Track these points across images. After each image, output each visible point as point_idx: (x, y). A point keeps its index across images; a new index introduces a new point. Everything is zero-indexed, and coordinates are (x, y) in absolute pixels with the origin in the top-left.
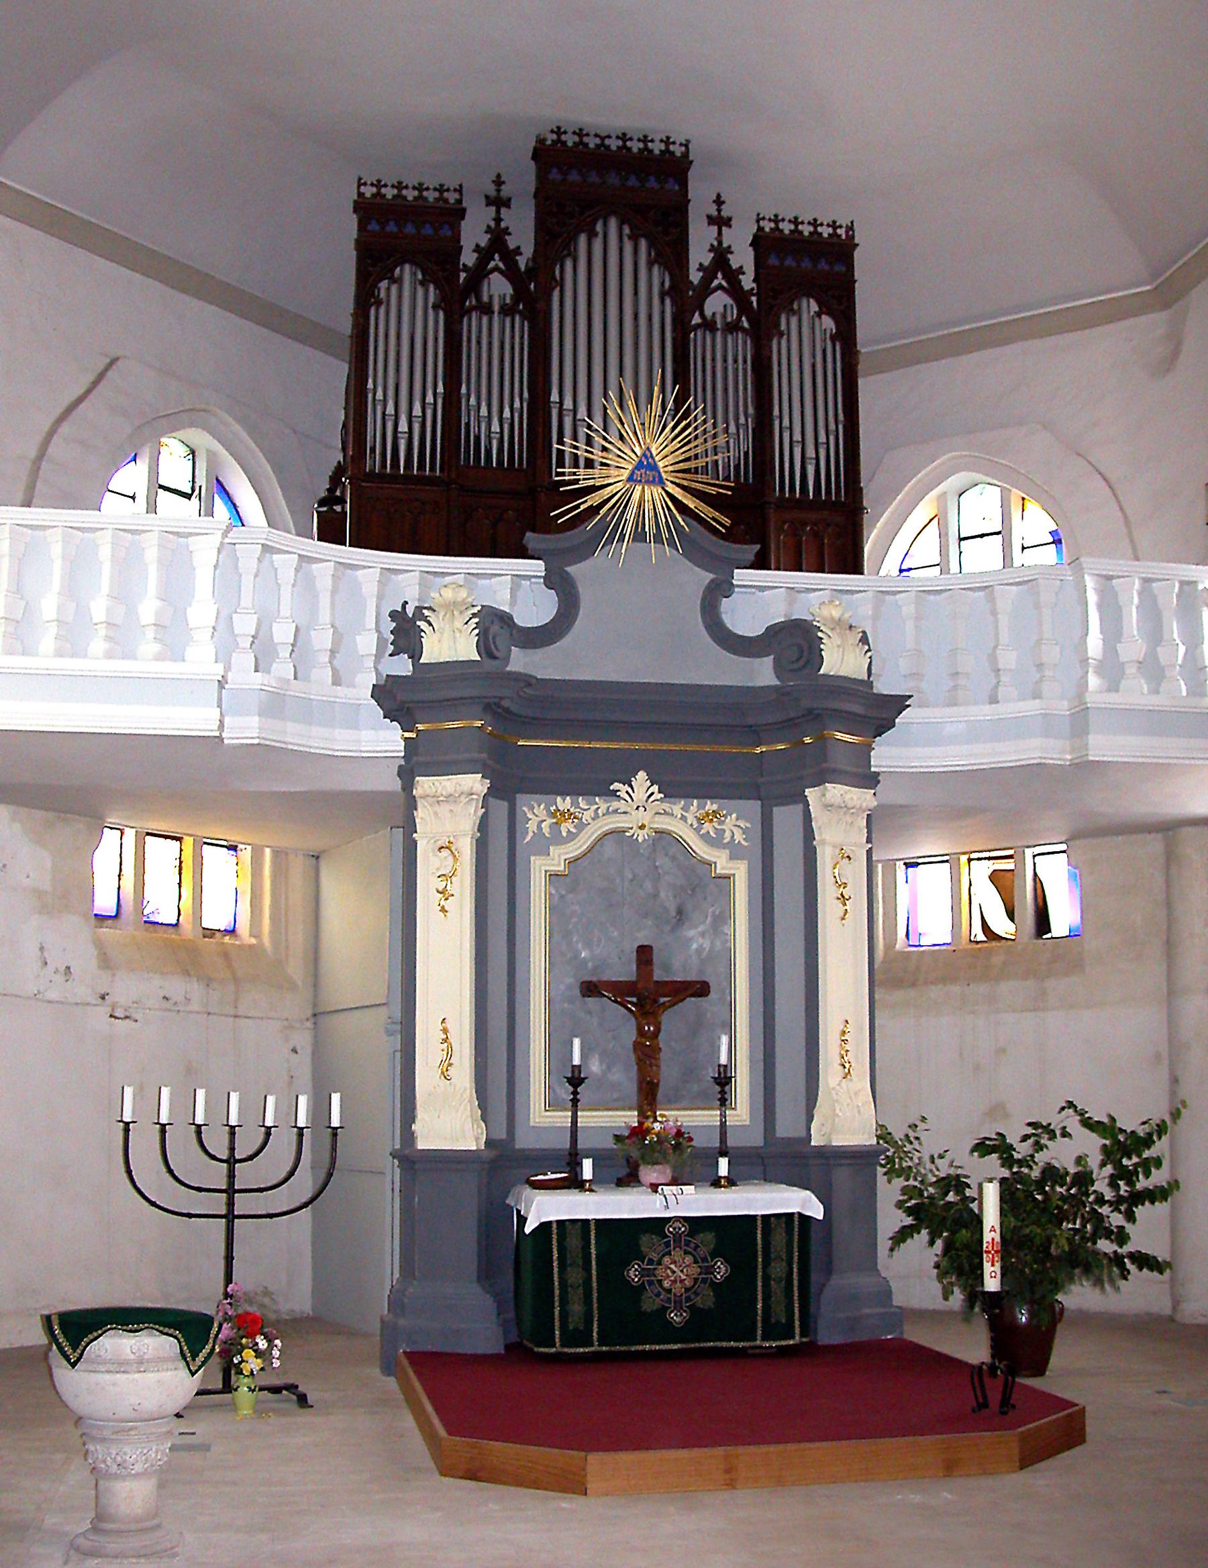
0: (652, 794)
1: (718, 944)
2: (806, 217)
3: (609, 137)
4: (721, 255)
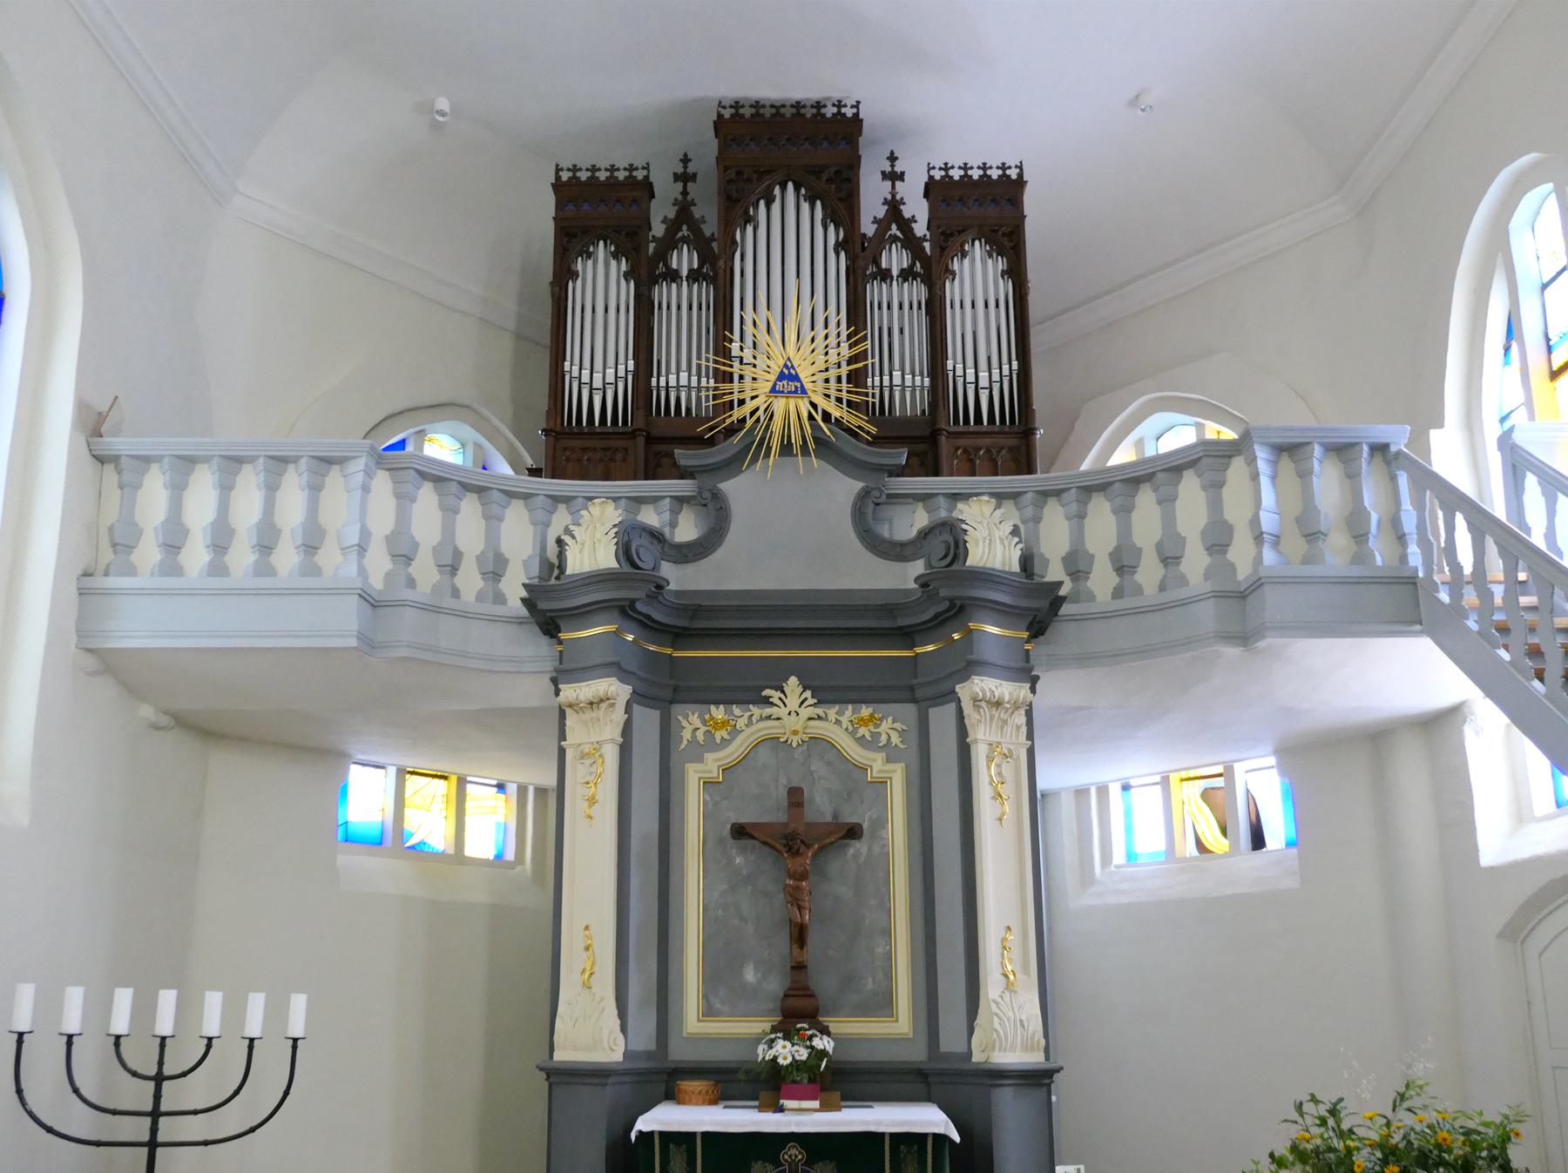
0: (806, 699)
2: (975, 162)
3: (784, 106)
4: (894, 205)
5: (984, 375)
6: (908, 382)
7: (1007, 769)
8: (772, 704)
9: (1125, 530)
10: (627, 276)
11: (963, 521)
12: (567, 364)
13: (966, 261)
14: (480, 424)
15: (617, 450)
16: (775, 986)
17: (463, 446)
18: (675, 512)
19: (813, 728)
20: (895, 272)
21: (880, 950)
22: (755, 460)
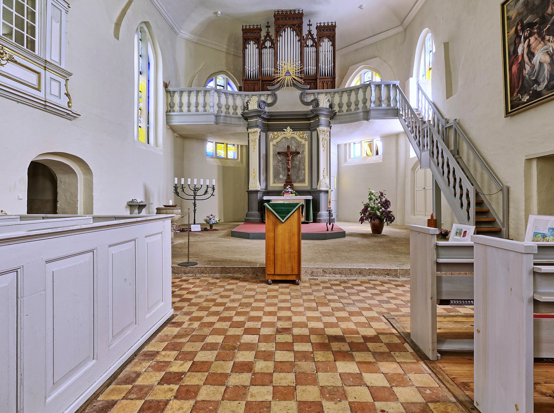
1: (303, 156)
4: (310, 32)
6: (312, 68)
9: (349, 99)
10: (257, 48)
11: (319, 99)
12: (246, 66)
13: (324, 43)
15: (256, 83)
16: (285, 178)
17: (224, 79)
18: (267, 97)
21: (303, 172)
22: (282, 87)
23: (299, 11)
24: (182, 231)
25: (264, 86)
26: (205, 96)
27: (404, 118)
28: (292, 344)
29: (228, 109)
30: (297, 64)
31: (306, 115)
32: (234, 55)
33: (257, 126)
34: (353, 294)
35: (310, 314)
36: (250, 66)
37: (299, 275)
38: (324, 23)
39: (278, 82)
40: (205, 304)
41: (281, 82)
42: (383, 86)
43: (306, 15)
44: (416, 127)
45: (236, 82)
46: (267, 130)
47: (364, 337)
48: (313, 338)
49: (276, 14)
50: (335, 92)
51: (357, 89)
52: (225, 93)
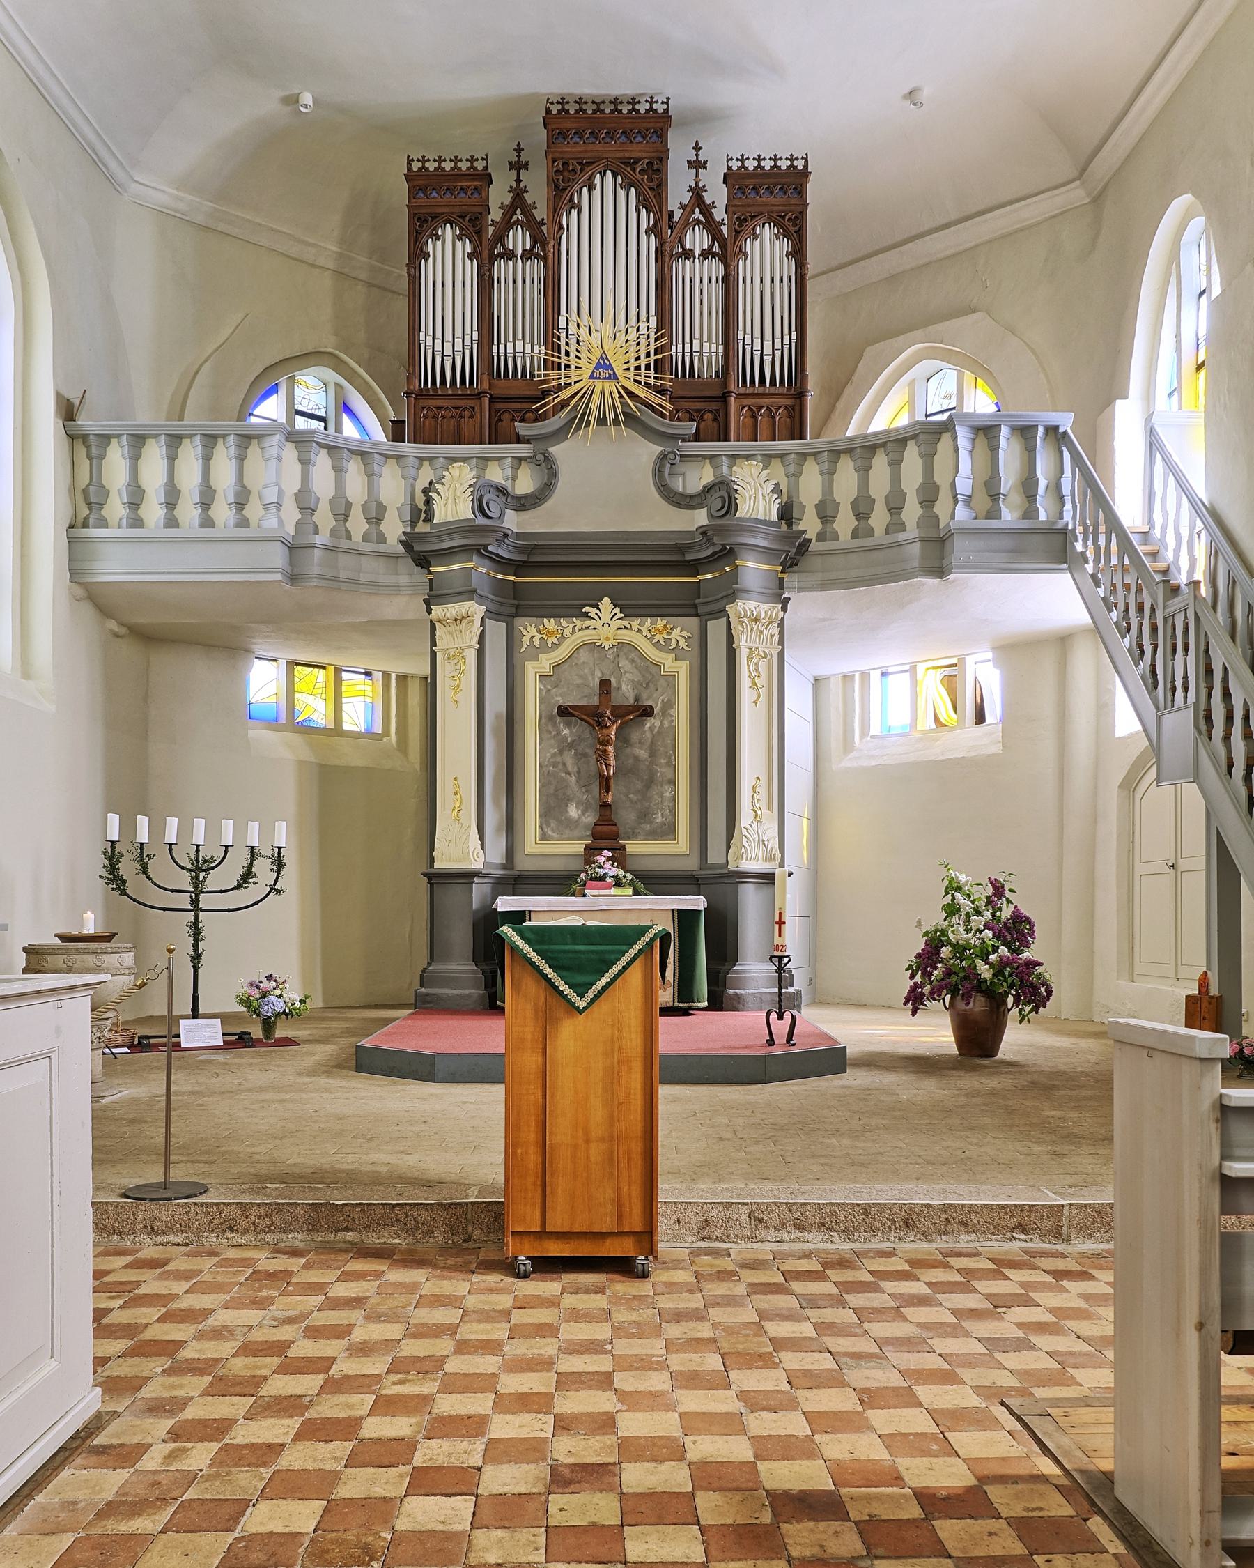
0: (616, 614)
1: (666, 724)
3: (603, 102)
4: (697, 193)
5: (768, 345)
7: (762, 666)
8: (591, 618)
9: (864, 483)
10: (470, 256)
11: (735, 483)
13: (757, 242)
14: (339, 366)
15: (465, 409)
16: (590, 819)
18: (515, 469)
19: (621, 635)
20: (697, 252)
21: (667, 794)
22: (578, 428)
23: (651, 103)
24: (141, 1045)
25: (499, 420)
26: (241, 458)
27: (1090, 568)
28: (617, 1533)
29: (342, 515)
30: (643, 330)
31: (680, 548)
32: (371, 285)
33: (470, 594)
34: (877, 1314)
35: (693, 1401)
36: (439, 335)
37: (647, 1237)
38: (759, 159)
39: (563, 405)
40: (240, 1366)
41: (576, 406)
42: (1005, 431)
43: (685, 123)
44: (1140, 608)
45: (379, 400)
46: (513, 610)
47: (924, 1497)
48: (711, 1507)
49: (554, 112)
50: (803, 456)
51: (895, 443)
52: (331, 449)
